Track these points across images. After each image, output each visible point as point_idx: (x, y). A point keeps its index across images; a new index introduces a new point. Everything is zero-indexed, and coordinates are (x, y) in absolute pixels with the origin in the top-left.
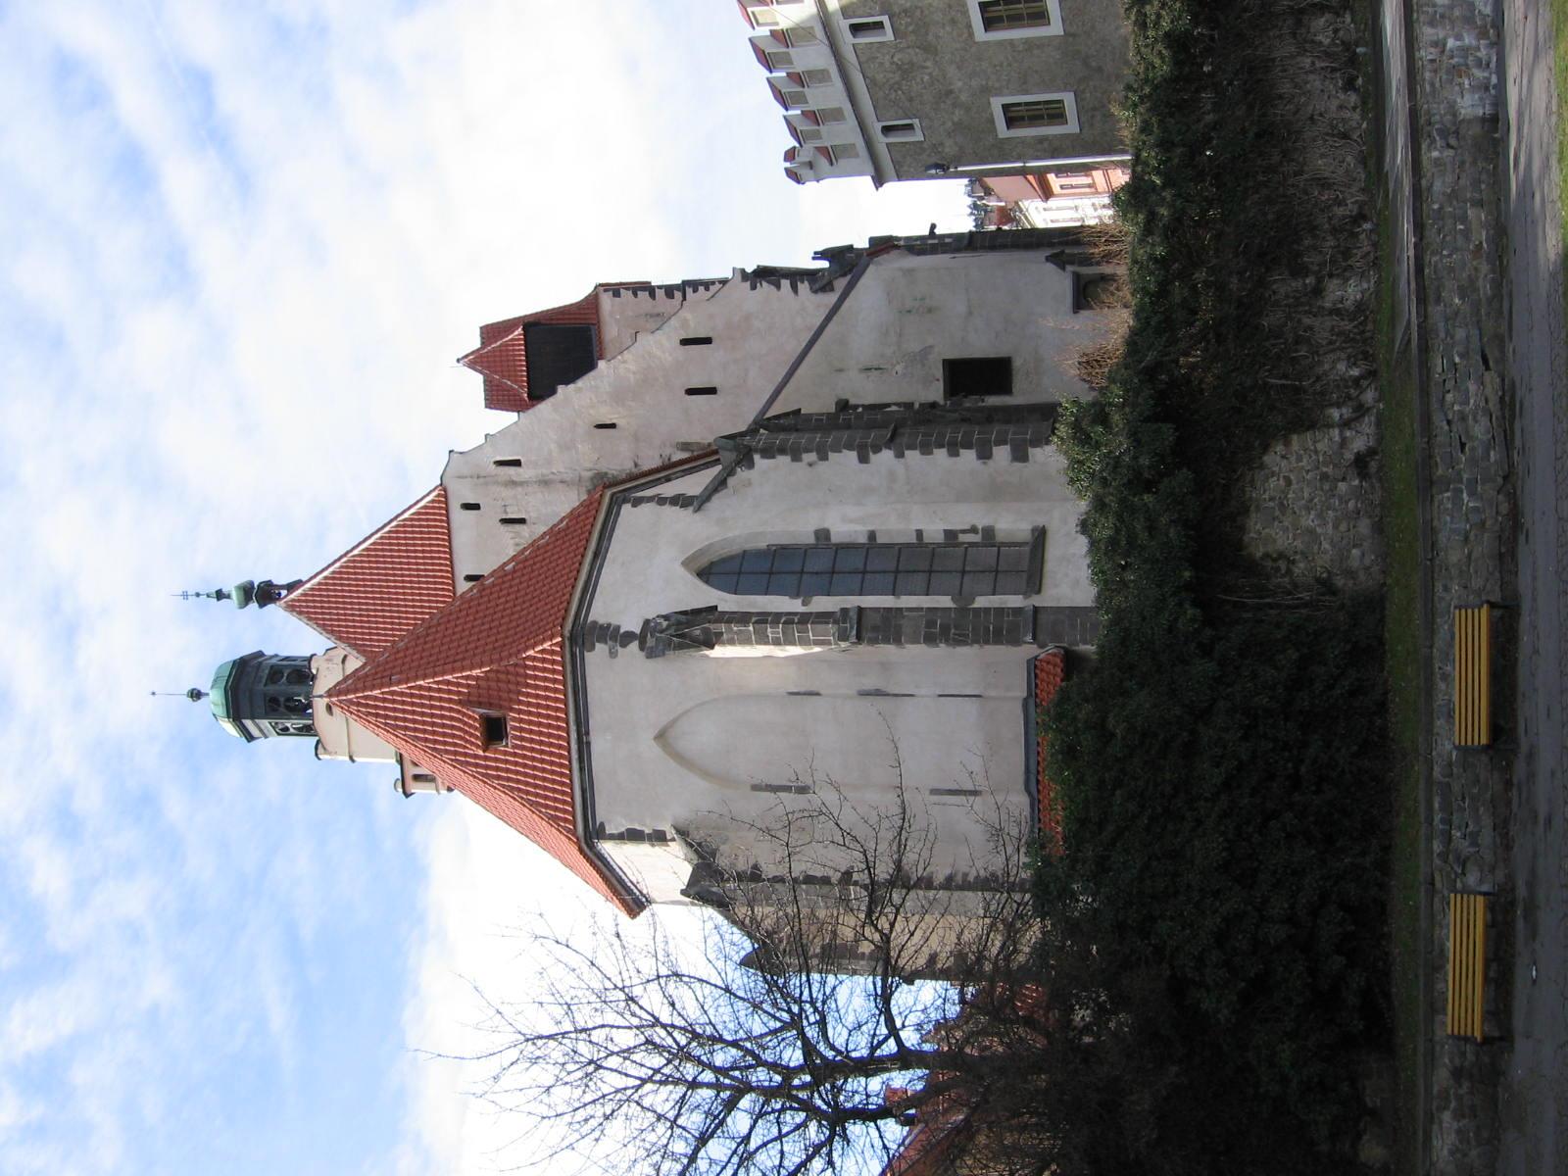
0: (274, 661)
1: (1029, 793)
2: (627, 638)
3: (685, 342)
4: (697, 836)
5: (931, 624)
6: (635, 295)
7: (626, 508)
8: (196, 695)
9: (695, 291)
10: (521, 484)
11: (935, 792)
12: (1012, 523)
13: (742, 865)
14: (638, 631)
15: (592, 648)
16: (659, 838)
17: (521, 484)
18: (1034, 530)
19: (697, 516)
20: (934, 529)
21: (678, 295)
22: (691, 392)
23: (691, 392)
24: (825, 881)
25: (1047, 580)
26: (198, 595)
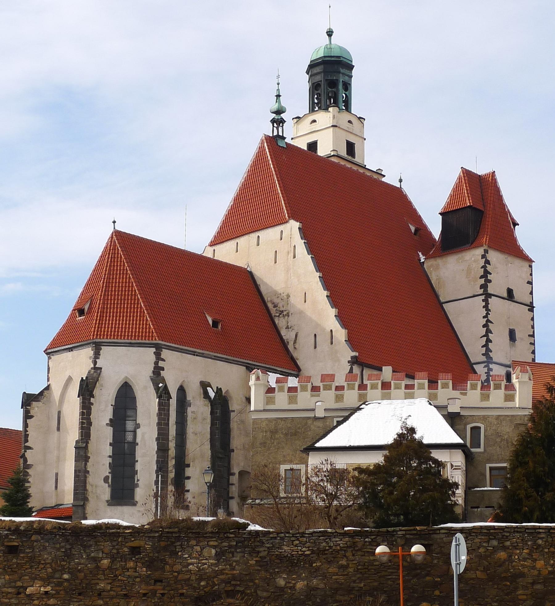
1: (55, 506)
2: (95, 363)
3: (331, 331)
4: (46, 393)
5: (80, 471)
6: (482, 268)
7: (154, 350)
8: (330, 33)
9: (483, 301)
11: (57, 474)
12: (140, 494)
13: (32, 413)
14: (97, 366)
15: (92, 350)
16: (48, 380)
18: (137, 502)
19: (149, 379)
20: (138, 467)
21: (481, 291)
22: (315, 335)
23: (315, 335)
24: (26, 441)
25: (113, 508)
26: (278, 84)
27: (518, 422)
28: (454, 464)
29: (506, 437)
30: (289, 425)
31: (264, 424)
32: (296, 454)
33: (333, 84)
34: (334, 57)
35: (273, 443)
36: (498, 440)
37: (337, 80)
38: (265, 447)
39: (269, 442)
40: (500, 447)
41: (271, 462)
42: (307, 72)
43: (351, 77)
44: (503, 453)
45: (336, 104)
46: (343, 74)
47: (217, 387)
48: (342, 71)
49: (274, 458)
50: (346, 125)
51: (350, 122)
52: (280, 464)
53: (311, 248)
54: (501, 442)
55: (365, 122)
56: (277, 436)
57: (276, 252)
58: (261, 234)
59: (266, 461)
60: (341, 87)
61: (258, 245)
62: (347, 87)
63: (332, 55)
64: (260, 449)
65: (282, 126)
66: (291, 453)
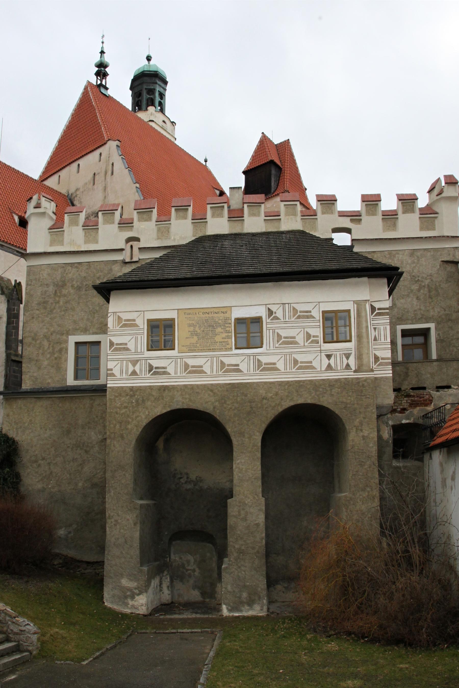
0: (158, 89)
8: (149, 59)
10: (105, 179)
17: (105, 179)
27: (443, 260)
28: (377, 305)
29: (427, 282)
30: (83, 274)
31: (45, 274)
32: (94, 317)
33: (151, 92)
34: (152, 71)
35: (58, 302)
36: (415, 287)
37: (155, 89)
38: (45, 308)
39: (51, 301)
40: (418, 298)
41: (54, 332)
42: (131, 88)
43: (165, 90)
44: (423, 308)
45: (153, 104)
46: (159, 85)
47: (16, 281)
48: (159, 82)
49: (59, 325)
50: (161, 124)
51: (164, 122)
52: (68, 333)
53: (131, 166)
54: (419, 290)
55: (176, 127)
56: (65, 291)
57: (95, 174)
58: (81, 162)
59: (46, 331)
60: (157, 94)
61: (78, 172)
62: (162, 96)
63: (151, 70)
64: (38, 312)
65: (105, 79)
66: (86, 317)
